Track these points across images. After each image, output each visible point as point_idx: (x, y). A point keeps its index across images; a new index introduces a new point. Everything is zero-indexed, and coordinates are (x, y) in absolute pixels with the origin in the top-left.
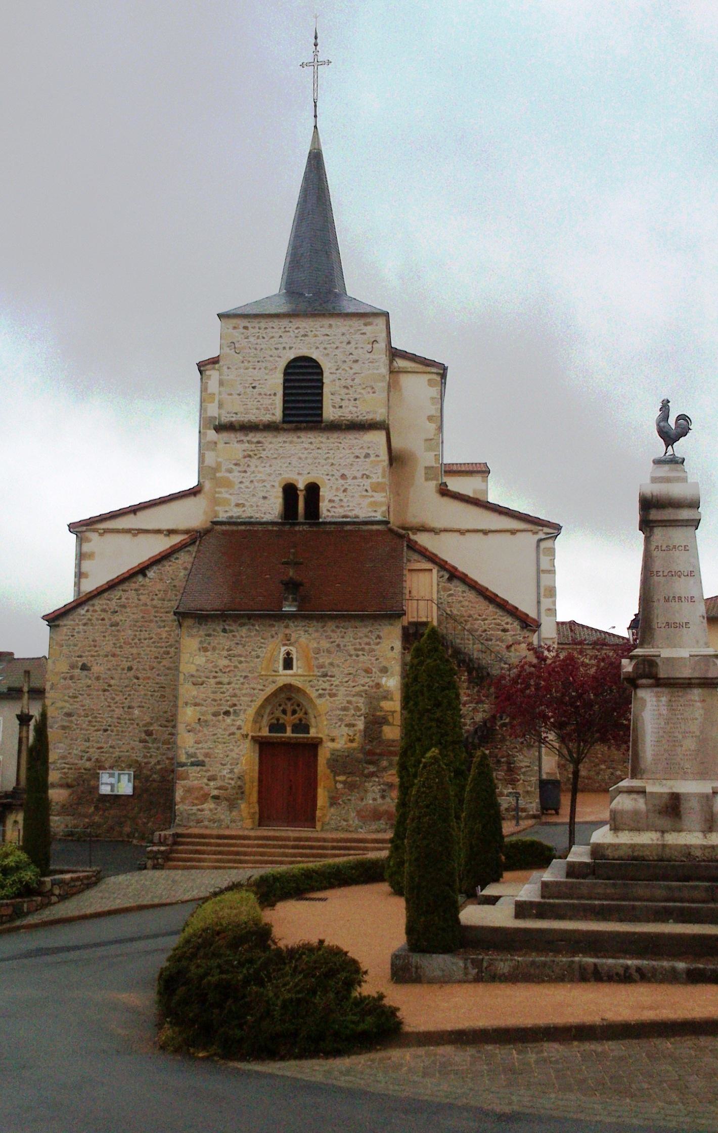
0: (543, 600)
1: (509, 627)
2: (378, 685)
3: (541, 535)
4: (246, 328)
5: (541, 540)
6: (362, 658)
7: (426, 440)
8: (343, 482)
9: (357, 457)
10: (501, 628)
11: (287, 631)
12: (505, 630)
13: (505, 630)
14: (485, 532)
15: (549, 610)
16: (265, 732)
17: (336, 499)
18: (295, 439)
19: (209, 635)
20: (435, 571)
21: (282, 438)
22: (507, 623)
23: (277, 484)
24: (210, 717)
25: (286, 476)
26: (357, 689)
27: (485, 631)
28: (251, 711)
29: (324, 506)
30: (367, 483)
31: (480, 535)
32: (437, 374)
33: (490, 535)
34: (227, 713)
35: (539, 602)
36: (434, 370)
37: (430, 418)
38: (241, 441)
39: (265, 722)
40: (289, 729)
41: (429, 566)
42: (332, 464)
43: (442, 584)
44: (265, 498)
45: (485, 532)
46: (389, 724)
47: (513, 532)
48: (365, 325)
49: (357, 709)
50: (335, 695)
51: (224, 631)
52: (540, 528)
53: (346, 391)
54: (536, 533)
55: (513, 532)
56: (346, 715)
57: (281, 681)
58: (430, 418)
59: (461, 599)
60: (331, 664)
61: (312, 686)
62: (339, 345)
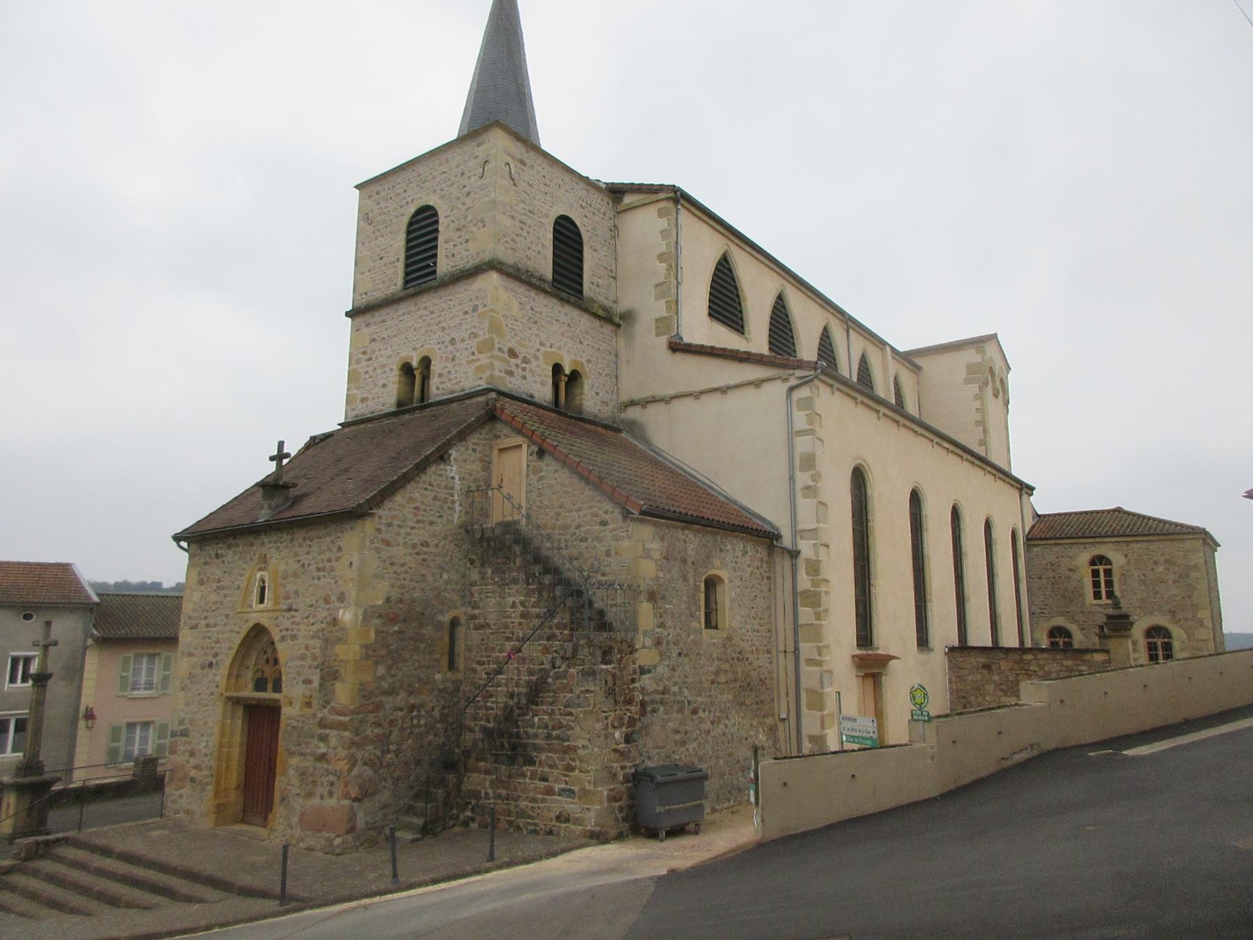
0: (798, 474)
1: (608, 517)
2: (335, 621)
3: (793, 382)
4: (378, 193)
5: (792, 389)
6: (323, 582)
7: (656, 286)
8: (451, 348)
9: (466, 313)
10: (599, 519)
11: (264, 550)
12: (604, 523)
13: (604, 523)
14: (724, 390)
15: (808, 488)
16: (248, 692)
17: (445, 372)
18: (413, 308)
19: (206, 563)
20: (525, 446)
21: (402, 308)
22: (606, 512)
23: (394, 367)
24: (198, 671)
25: (403, 354)
26: (315, 628)
27: (579, 527)
28: (228, 662)
29: (434, 382)
30: (474, 343)
31: (718, 395)
32: (668, 199)
33: (730, 393)
34: (211, 665)
35: (792, 478)
36: (662, 196)
37: (661, 257)
38: (368, 325)
39: (249, 675)
40: (270, 685)
41: (517, 440)
42: (443, 329)
43: (532, 464)
44: (384, 386)
45: (724, 390)
46: (344, 682)
47: (757, 384)
48: (478, 146)
49: (314, 657)
50: (294, 638)
51: (217, 556)
52: (791, 372)
53: (458, 234)
54: (786, 380)
55: (757, 384)
56: (303, 666)
57: (254, 619)
58: (661, 257)
59: (552, 482)
60: (296, 592)
61: (277, 625)
62: (453, 179)
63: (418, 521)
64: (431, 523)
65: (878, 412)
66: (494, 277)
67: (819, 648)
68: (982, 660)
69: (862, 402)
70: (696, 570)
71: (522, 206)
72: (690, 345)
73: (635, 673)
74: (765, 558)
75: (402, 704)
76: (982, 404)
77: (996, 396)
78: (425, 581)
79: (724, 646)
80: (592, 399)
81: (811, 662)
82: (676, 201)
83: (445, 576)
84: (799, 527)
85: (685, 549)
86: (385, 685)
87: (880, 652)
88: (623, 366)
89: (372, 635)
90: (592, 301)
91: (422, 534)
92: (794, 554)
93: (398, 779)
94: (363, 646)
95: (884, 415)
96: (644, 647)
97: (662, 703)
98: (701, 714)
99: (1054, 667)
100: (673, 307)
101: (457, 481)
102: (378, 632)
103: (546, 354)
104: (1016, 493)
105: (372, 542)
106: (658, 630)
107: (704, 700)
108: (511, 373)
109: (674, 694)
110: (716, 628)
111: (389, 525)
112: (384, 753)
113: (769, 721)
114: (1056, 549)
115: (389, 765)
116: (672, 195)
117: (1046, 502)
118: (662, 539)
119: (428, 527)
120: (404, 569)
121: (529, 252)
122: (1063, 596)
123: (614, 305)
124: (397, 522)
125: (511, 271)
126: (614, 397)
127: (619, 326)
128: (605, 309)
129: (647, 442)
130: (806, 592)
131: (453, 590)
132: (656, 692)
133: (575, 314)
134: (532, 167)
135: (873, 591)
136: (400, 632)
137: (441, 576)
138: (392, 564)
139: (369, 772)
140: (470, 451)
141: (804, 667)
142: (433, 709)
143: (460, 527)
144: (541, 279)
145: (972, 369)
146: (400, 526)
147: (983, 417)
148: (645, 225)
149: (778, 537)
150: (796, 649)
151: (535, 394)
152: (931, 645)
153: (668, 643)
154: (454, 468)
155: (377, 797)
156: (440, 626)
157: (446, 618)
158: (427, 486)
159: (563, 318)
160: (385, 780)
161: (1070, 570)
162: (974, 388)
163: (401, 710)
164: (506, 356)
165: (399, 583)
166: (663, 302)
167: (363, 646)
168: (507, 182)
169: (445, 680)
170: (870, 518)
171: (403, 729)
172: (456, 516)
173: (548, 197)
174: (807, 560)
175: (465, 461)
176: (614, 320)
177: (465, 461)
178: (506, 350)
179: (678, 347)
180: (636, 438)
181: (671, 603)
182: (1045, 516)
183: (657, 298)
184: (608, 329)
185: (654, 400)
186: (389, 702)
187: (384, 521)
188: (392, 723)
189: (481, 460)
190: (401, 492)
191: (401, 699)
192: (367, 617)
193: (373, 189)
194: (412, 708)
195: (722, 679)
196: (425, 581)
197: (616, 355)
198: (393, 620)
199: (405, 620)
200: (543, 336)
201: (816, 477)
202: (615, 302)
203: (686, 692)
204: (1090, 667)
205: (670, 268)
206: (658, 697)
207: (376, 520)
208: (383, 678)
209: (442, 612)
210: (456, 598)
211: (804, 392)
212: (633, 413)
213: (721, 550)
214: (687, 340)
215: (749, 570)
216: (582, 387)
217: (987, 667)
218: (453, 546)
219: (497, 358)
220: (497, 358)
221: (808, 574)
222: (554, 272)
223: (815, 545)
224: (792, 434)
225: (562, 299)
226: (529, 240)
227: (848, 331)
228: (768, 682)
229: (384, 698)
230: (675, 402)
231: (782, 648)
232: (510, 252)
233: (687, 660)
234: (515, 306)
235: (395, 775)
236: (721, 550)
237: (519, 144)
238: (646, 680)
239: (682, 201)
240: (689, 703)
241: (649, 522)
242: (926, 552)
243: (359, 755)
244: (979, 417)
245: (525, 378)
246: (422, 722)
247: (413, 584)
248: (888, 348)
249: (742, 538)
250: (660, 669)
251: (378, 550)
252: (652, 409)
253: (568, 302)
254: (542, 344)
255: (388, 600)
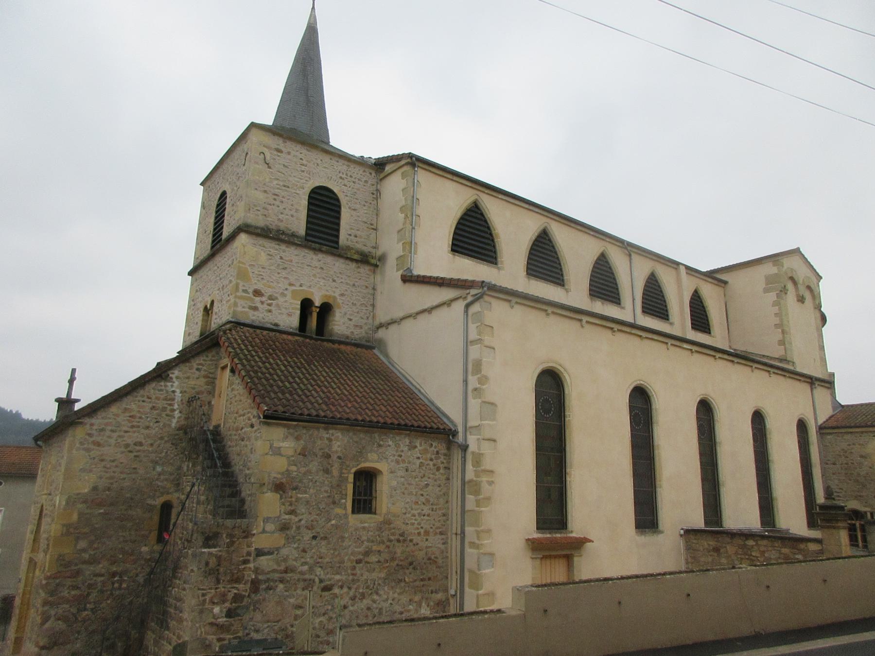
0: (470, 377)
3: (470, 299)
7: (399, 232)
14: (430, 310)
15: (476, 389)
32: (407, 164)
33: (434, 312)
35: (466, 381)
36: (403, 162)
37: (402, 210)
45: (430, 310)
47: (448, 303)
52: (468, 291)
63: (133, 427)
64: (148, 427)
65: (580, 320)
66: (243, 238)
67: (478, 532)
68: (713, 543)
69: (553, 313)
70: (342, 464)
71: (275, 182)
72: (418, 276)
73: (249, 554)
74: (444, 451)
75: (103, 571)
76: (780, 309)
77: (801, 300)
78: (137, 473)
79: (380, 529)
80: (341, 324)
81: (473, 545)
82: (413, 165)
83: (159, 469)
84: (469, 424)
85: (330, 447)
86: (86, 556)
87: (574, 535)
88: (379, 297)
89: (75, 517)
90: (349, 248)
91: (136, 436)
92: (465, 448)
93: (93, 632)
94: (64, 525)
95: (588, 322)
96: (264, 531)
97: (281, 582)
98: (336, 590)
99: (773, 555)
100: (408, 247)
101: (178, 394)
102: (80, 515)
103: (293, 292)
104: (807, 387)
105: (81, 443)
106: (287, 517)
107: (344, 578)
108: (255, 309)
109: (302, 573)
110: (375, 513)
111: (102, 430)
112: (79, 610)
113: (440, 596)
114: (847, 437)
115: (84, 621)
116: (409, 160)
117: (849, 393)
118: (298, 438)
119: (143, 431)
120: (114, 464)
121: (281, 217)
122: (857, 481)
123: (373, 251)
124: (110, 428)
125: (259, 231)
126: (370, 321)
127: (377, 266)
128: (358, 252)
129: (387, 356)
130: (470, 481)
131: (166, 480)
132: (274, 571)
133: (329, 259)
134: (289, 153)
135: (568, 479)
136: (105, 514)
137: (154, 469)
138: (102, 460)
139: (61, 625)
140: (194, 370)
141: (468, 550)
142: (137, 575)
143: (179, 429)
144: (293, 235)
145: (770, 280)
146: (112, 431)
147: (781, 320)
148: (395, 185)
149: (455, 434)
150: (463, 532)
151: (281, 324)
152: (661, 527)
153: (298, 528)
154: (176, 384)
155: (68, 646)
156: (151, 508)
157: (159, 502)
158: (145, 399)
159: (315, 263)
160: (78, 632)
161: (862, 456)
162: (772, 296)
163: (102, 575)
164: (251, 295)
165: (108, 475)
166: (401, 244)
167: (64, 525)
168: (262, 167)
169: (152, 552)
170: (567, 413)
171: (102, 592)
172: (175, 421)
173: (305, 174)
174: (473, 453)
175: (188, 378)
176: (368, 260)
177: (188, 378)
178: (251, 291)
179: (409, 279)
180: (381, 352)
181: (305, 492)
182: (848, 406)
183: (399, 241)
184: (365, 270)
185: (393, 322)
186: (88, 570)
187: (95, 427)
188: (90, 586)
189: (205, 377)
190: (118, 404)
191: (100, 568)
192: (70, 502)
193: (208, 184)
194: (114, 574)
195: (373, 558)
196: (137, 473)
197: (374, 289)
198: (100, 505)
199: (112, 504)
200: (292, 279)
201: (484, 380)
202: (374, 248)
203: (318, 571)
204: (804, 556)
205: (406, 217)
206: (276, 576)
207: (88, 426)
208: (84, 550)
209: (153, 498)
210: (169, 485)
211: (476, 308)
212: (381, 333)
213: (380, 446)
214: (416, 272)
215: (418, 462)
216: (334, 316)
217: (717, 550)
218: (169, 445)
219: (241, 298)
220: (241, 298)
221: (473, 466)
222: (307, 228)
223: (478, 439)
224: (467, 343)
225: (314, 249)
226: (281, 207)
227: (630, 255)
228: (440, 561)
229: (84, 566)
230: (404, 323)
231: (454, 531)
232: (261, 217)
233: (324, 543)
234: (263, 257)
235: (91, 629)
236: (380, 446)
237: (276, 138)
238: (264, 562)
239: (417, 163)
240: (321, 581)
241: (277, 424)
242: (656, 443)
243: (53, 612)
244: (777, 321)
245: (270, 311)
246: (124, 585)
247: (122, 476)
248: (682, 268)
249: (409, 435)
250: (284, 552)
251: (88, 450)
252: (393, 328)
253: (320, 251)
254: (291, 285)
255: (95, 488)
